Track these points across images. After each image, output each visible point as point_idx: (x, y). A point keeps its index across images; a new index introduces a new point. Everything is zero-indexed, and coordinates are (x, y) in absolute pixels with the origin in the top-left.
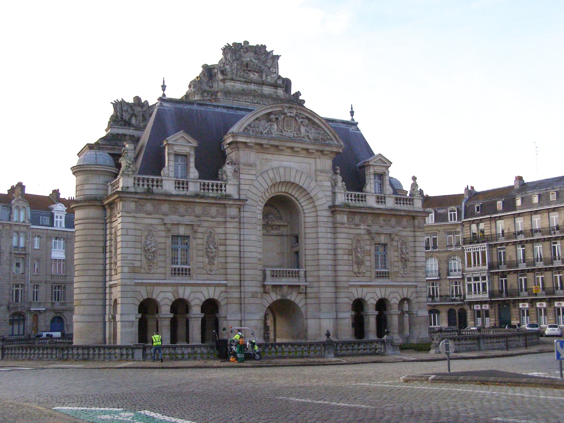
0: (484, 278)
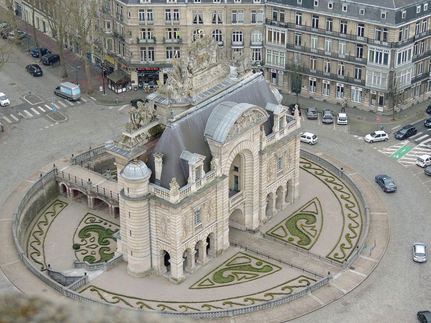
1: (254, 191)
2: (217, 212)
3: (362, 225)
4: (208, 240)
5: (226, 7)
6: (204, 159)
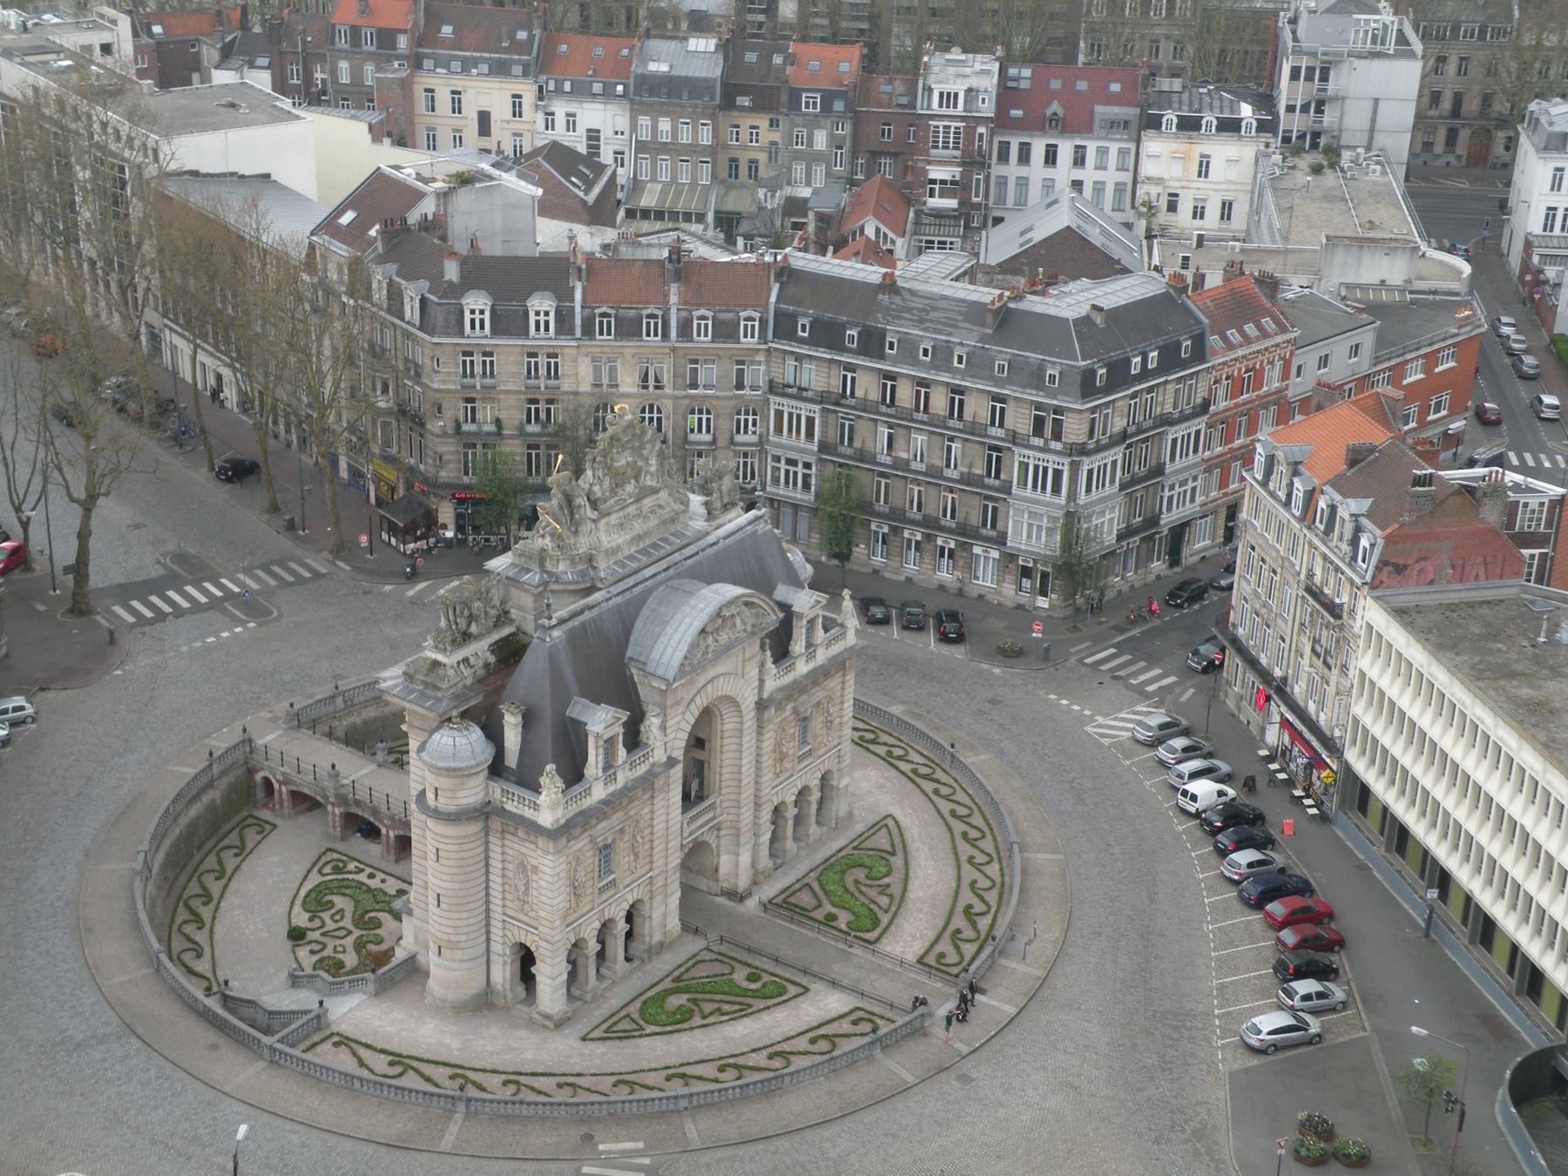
0: (807, 466)
1: (743, 796)
2: (652, 848)
3: (1003, 885)
4: (629, 918)
5: (674, 349)
6: (625, 719)
